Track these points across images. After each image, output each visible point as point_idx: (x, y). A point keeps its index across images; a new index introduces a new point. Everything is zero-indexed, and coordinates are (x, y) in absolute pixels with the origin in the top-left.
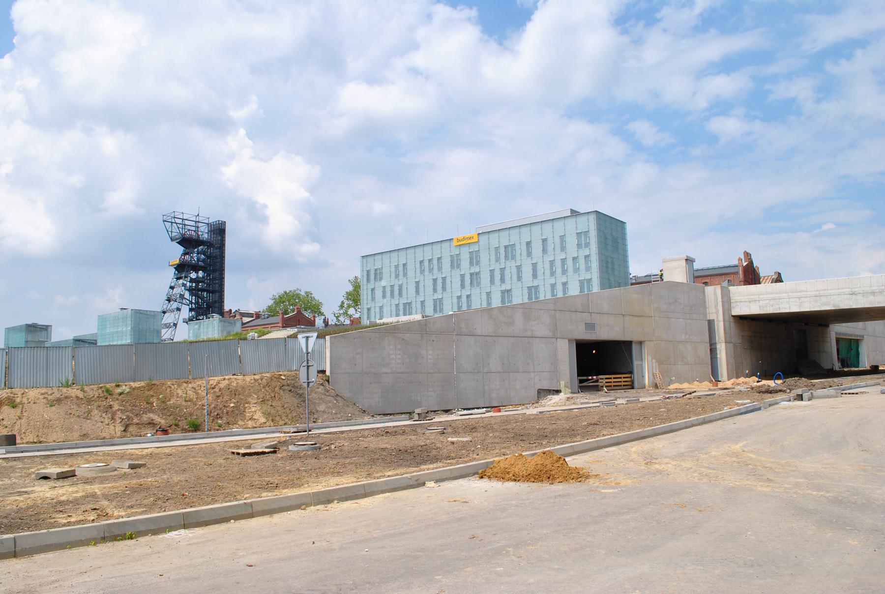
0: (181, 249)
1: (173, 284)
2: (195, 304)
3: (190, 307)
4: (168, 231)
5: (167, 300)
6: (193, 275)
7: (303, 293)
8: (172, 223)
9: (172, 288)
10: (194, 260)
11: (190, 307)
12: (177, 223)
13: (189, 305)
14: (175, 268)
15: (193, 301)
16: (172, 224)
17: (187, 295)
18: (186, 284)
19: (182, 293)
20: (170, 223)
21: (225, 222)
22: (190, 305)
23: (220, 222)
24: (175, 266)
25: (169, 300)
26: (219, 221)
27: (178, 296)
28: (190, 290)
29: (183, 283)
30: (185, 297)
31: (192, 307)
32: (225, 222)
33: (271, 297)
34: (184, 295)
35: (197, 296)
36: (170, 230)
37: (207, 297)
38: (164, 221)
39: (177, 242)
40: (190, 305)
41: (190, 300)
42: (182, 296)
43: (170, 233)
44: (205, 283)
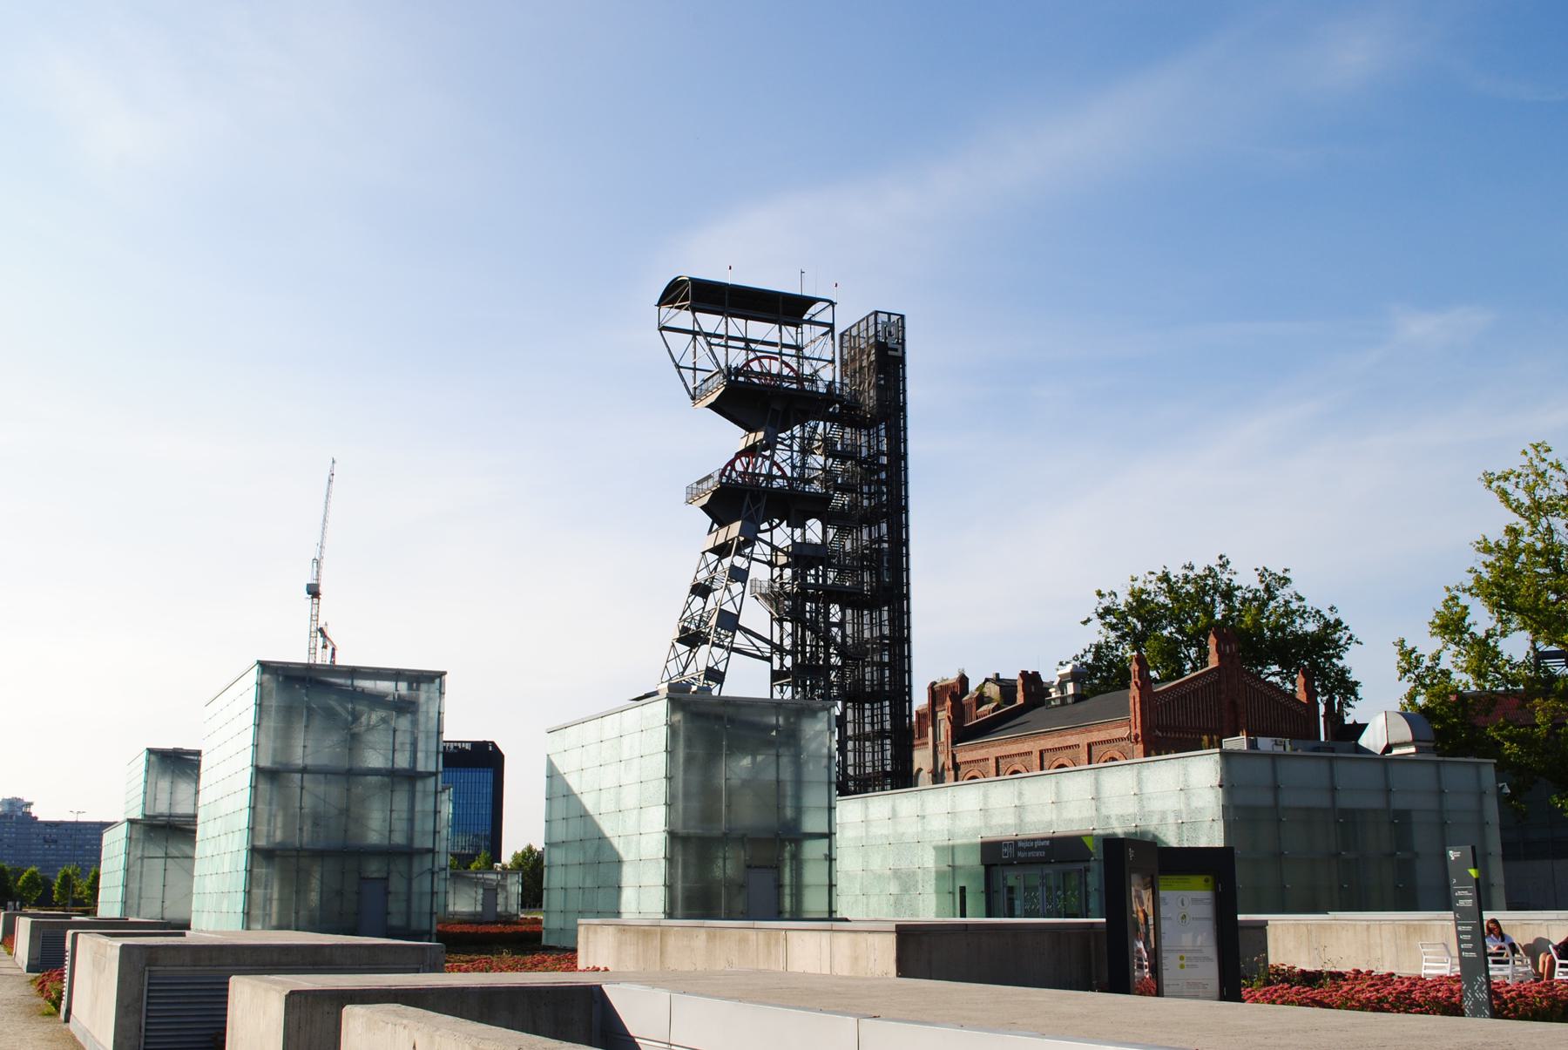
0: (732, 438)
1: (703, 576)
2: (793, 653)
3: (776, 667)
4: (678, 367)
5: (679, 640)
6: (783, 536)
7: (1246, 579)
8: (694, 333)
9: (702, 590)
10: (784, 476)
11: (776, 667)
12: (707, 335)
13: (770, 659)
14: (703, 508)
15: (787, 643)
16: (695, 339)
17: (757, 616)
18: (746, 573)
19: (729, 608)
20: (691, 336)
21: (902, 317)
22: (776, 659)
23: (883, 318)
24: (705, 500)
25: (691, 638)
26: (876, 313)
27: (713, 622)
28: (773, 598)
29: (733, 567)
30: (741, 622)
31: (782, 665)
32: (902, 317)
33: (1093, 605)
34: (737, 617)
35: (796, 616)
36: (687, 361)
37: (841, 625)
38: (663, 328)
39: (711, 406)
40: (776, 659)
41: (776, 640)
42: (729, 621)
43: (688, 374)
44: (831, 565)
